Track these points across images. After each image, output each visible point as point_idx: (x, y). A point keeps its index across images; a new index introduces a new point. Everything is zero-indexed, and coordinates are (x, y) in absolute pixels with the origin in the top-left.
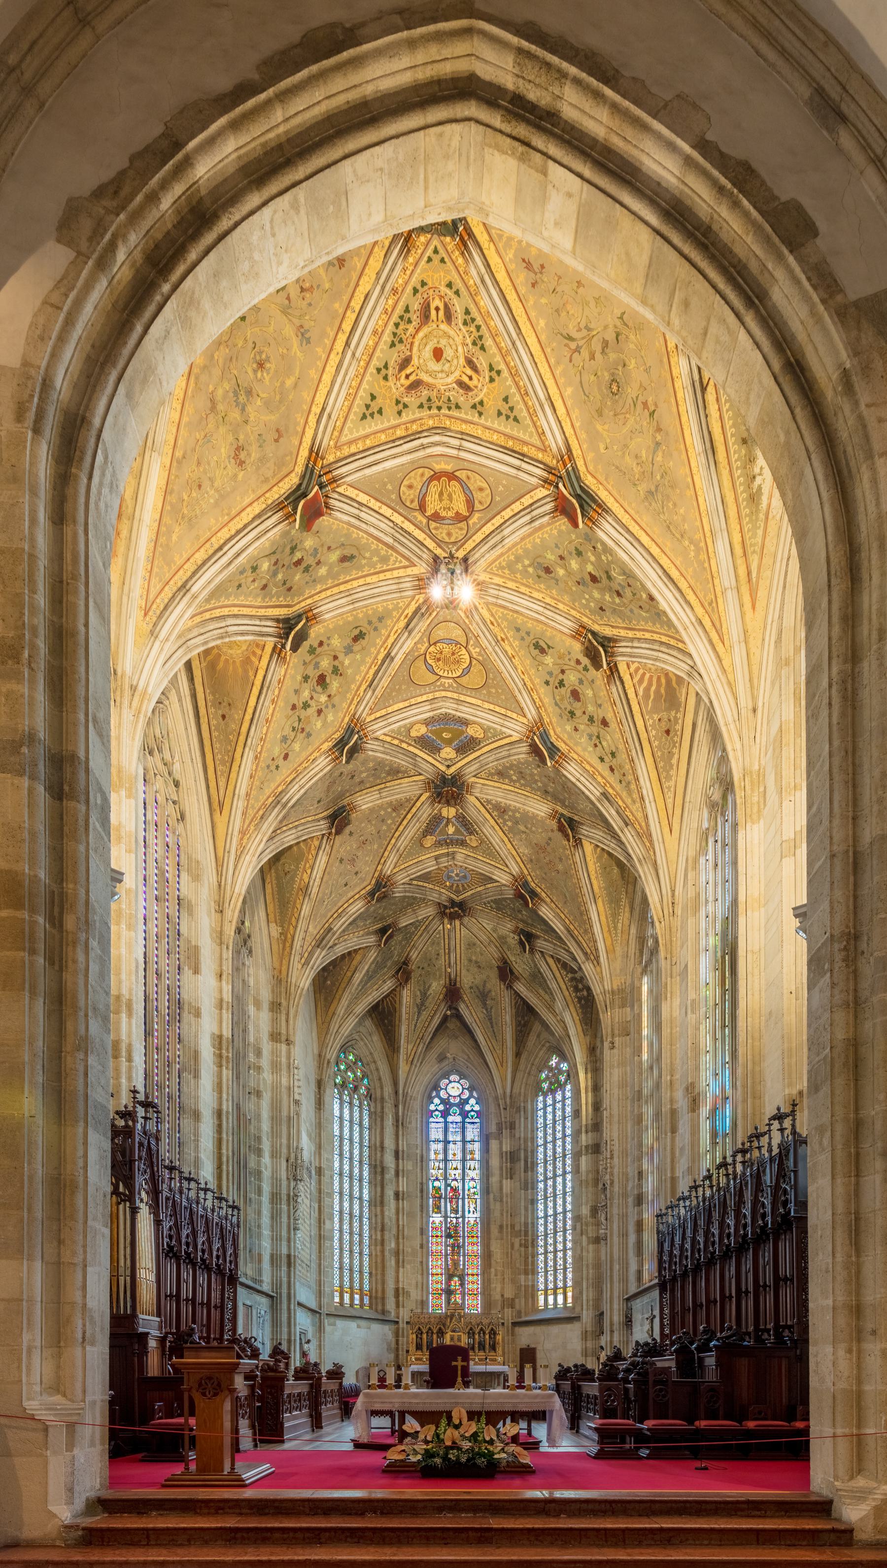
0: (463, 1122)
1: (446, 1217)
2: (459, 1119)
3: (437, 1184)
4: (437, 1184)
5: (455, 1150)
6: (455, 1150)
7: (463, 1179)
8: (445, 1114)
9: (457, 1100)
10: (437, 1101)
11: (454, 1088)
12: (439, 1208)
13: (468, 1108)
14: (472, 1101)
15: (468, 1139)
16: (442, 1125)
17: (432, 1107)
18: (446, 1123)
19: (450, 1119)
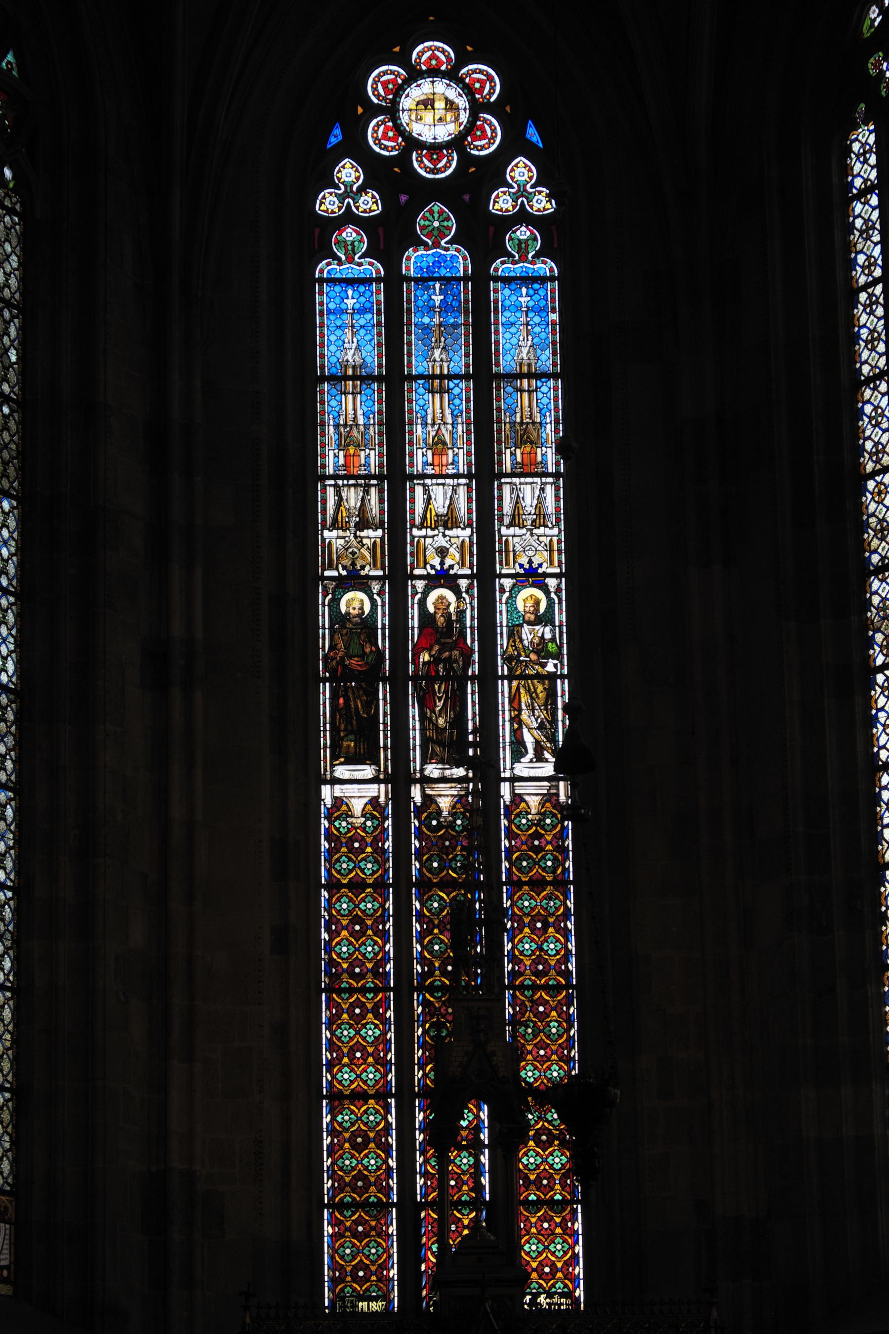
0: (480, 279)
1: (399, 779)
2: (459, 261)
3: (354, 601)
4: (354, 601)
5: (439, 417)
6: (439, 417)
7: (485, 577)
8: (390, 237)
9: (449, 166)
10: (348, 172)
11: (432, 108)
12: (366, 730)
13: (502, 203)
14: (521, 170)
15: (506, 363)
16: (377, 295)
17: (328, 203)
18: (394, 282)
19: (414, 261)
